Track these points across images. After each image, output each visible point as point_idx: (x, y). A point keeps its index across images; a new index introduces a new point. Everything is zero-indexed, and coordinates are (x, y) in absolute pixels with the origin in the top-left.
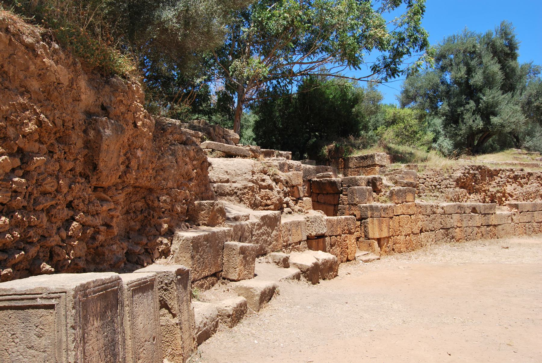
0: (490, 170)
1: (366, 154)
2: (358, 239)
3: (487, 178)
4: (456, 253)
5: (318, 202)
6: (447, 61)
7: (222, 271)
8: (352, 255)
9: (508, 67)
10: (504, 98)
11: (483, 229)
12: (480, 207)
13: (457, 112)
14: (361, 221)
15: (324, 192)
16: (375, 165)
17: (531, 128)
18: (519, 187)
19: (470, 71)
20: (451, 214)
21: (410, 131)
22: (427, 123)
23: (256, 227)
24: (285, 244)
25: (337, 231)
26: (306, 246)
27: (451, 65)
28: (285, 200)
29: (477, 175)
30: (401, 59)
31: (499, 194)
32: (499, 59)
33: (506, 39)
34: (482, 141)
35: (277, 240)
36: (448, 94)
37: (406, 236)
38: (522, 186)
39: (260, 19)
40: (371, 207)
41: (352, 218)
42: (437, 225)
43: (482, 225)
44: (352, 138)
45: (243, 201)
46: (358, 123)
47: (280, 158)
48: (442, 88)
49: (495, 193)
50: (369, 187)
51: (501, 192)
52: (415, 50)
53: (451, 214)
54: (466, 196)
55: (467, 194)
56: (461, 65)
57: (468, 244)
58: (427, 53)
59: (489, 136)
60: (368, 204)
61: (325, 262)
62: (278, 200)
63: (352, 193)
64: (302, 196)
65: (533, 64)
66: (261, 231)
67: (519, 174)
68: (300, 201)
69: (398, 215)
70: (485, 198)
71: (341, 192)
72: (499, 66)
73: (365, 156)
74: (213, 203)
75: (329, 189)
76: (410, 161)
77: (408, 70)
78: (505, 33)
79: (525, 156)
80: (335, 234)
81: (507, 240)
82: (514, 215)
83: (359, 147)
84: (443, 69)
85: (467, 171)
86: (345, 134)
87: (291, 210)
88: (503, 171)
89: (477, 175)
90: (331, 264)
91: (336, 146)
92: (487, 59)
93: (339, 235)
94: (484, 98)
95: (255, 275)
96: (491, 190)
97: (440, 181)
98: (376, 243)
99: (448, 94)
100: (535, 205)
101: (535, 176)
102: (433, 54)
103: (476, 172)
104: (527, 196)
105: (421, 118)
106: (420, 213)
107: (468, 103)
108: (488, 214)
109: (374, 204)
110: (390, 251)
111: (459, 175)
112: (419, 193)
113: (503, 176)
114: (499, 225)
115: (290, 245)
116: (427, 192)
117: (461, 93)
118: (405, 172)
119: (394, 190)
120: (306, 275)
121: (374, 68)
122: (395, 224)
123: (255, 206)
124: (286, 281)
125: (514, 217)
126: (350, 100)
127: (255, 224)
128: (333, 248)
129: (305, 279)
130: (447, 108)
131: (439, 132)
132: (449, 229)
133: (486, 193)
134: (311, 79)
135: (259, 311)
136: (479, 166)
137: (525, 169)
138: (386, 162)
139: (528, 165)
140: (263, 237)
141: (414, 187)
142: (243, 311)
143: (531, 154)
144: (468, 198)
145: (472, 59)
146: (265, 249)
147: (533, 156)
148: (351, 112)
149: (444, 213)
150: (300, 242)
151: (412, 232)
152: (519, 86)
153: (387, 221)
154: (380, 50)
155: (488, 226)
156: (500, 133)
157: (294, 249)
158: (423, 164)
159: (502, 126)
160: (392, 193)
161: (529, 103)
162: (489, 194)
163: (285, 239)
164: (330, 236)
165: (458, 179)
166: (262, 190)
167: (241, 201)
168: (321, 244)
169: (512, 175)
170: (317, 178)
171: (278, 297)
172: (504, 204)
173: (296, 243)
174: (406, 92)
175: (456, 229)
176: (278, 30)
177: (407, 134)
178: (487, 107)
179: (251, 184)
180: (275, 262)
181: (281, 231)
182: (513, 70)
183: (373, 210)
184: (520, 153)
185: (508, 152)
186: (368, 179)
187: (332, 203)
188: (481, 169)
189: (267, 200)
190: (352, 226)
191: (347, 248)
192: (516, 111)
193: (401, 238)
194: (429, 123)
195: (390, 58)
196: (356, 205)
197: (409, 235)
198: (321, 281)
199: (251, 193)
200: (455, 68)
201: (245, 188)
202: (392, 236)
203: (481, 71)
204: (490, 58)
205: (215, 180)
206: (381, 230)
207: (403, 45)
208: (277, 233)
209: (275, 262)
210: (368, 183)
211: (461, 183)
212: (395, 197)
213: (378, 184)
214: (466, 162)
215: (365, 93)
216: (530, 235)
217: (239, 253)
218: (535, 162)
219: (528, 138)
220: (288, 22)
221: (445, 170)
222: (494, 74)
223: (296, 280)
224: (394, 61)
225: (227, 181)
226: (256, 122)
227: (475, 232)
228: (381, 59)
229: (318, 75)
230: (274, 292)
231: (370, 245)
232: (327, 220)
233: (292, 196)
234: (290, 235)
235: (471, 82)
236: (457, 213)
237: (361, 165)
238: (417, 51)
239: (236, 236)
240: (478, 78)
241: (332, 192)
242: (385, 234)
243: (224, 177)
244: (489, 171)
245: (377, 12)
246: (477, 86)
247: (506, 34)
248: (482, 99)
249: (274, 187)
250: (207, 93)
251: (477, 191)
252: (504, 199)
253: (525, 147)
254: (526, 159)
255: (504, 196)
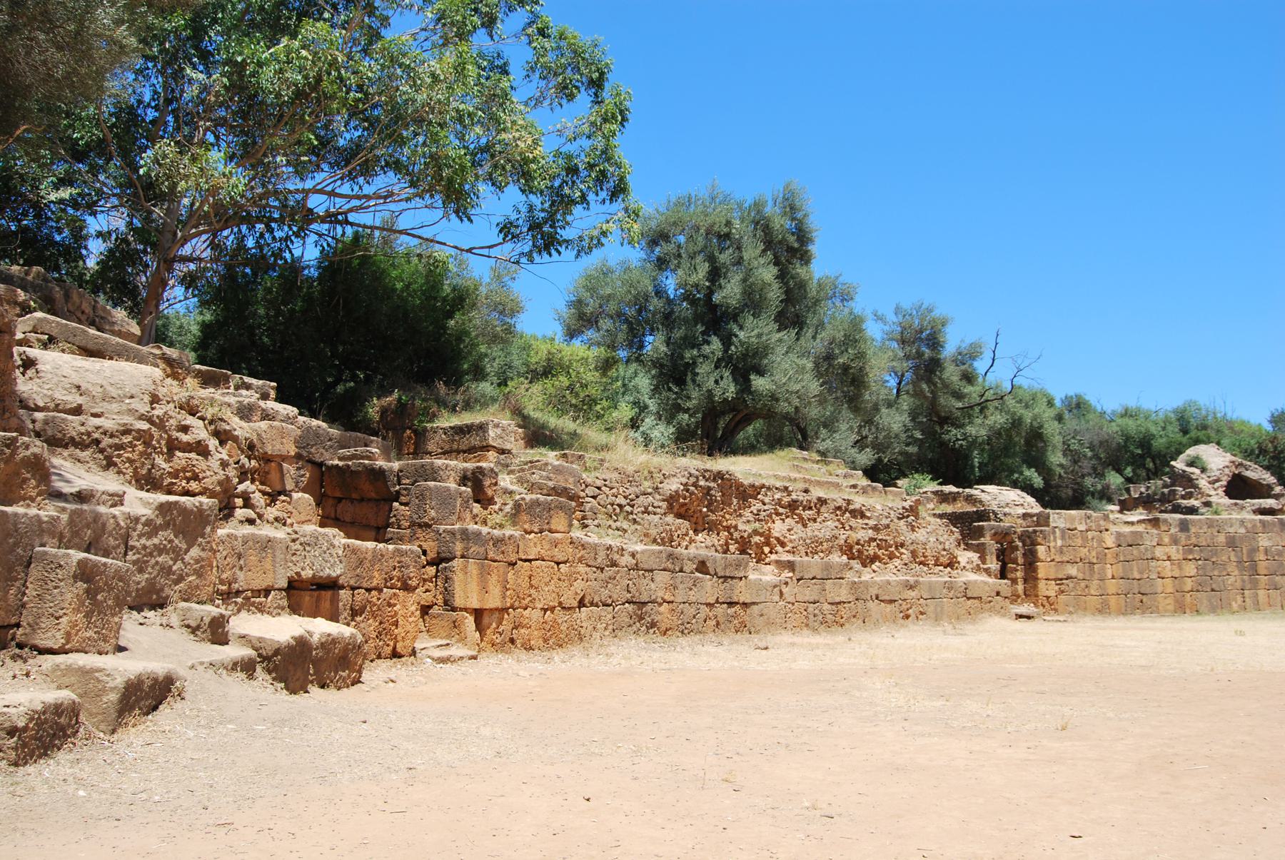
0: (742, 485)
1: (469, 422)
2: (425, 610)
3: (735, 501)
4: (656, 655)
5: (337, 519)
6: (671, 248)
7: (18, 625)
8: (408, 642)
9: (792, 277)
10: (780, 340)
11: (720, 610)
12: (715, 561)
13: (682, 358)
14: (438, 565)
15: (354, 496)
16: (487, 448)
17: (832, 413)
18: (800, 526)
19: (715, 274)
20: (652, 571)
21: (582, 395)
22: (619, 383)
23: (140, 527)
24: (224, 588)
25: (372, 578)
26: (285, 603)
27: (679, 256)
28: (241, 488)
29: (713, 492)
30: (569, 218)
31: (757, 539)
32: (776, 257)
33: (793, 219)
34: (732, 431)
35: (199, 574)
36: (668, 319)
37: (545, 610)
38: (805, 526)
39: (239, 59)
40: (464, 532)
41: (412, 552)
42: (618, 592)
43: (717, 602)
44: (442, 388)
45: (115, 465)
46: (458, 356)
47: (244, 392)
48: (655, 304)
49: (750, 536)
50: (463, 488)
51: (761, 535)
52: (600, 198)
53: (652, 571)
54: (687, 535)
55: (691, 532)
56: (699, 258)
57: (683, 641)
58: (626, 210)
59: (747, 420)
60: (457, 526)
61: (329, 643)
62: (220, 483)
63: (422, 497)
64: (289, 485)
65: (841, 279)
66: (156, 541)
67: (801, 498)
68: (282, 498)
69: (530, 561)
70: (727, 544)
71: (396, 497)
72: (774, 270)
73: (467, 426)
74: (15, 440)
75: (368, 489)
76: (570, 447)
77: (581, 238)
78: (791, 208)
79: (815, 466)
80: (365, 585)
81: (769, 637)
82: (786, 583)
83: (455, 406)
84: (662, 263)
85: (692, 480)
86: (426, 378)
87: (254, 516)
88: (769, 489)
89: (713, 492)
90: (346, 650)
91: (400, 399)
92: (752, 251)
93: (375, 589)
94: (742, 335)
95: (121, 649)
96: (741, 527)
97: (632, 496)
98: (470, 620)
99: (668, 319)
100: (828, 567)
101: (832, 506)
102: (637, 216)
103: (712, 485)
104: (814, 547)
105: (606, 366)
106: (580, 561)
107: (708, 343)
108: (732, 578)
109: (472, 527)
110: (503, 644)
111: (674, 487)
112: (584, 518)
113: (767, 500)
114: (754, 603)
115: (238, 593)
116: (602, 519)
117: (697, 319)
118: (554, 467)
119: (523, 499)
120: (271, 666)
121: (505, 226)
122: (520, 581)
123: (149, 482)
124: (211, 672)
125: (785, 590)
126: (444, 299)
127: (137, 520)
128: (358, 619)
129: (268, 677)
130: (663, 348)
131: (646, 407)
132: (645, 603)
133: (731, 534)
134: (357, 236)
135: (113, 731)
136: (719, 472)
137: (811, 489)
138: (514, 442)
139: (819, 483)
140: (160, 559)
141: (571, 498)
142: (63, 729)
143: (827, 463)
144: (692, 541)
145: (722, 250)
146: (162, 590)
147: (830, 468)
148: (445, 328)
149: (636, 567)
150: (267, 592)
151: (560, 603)
152: (811, 320)
153: (502, 570)
154: (523, 191)
155: (731, 604)
156: (769, 415)
157: (248, 605)
158: (598, 456)
159: (774, 398)
160: (517, 506)
161: (829, 357)
162: (736, 535)
163: (224, 576)
164: (353, 589)
165: (671, 497)
166: (178, 454)
167: (109, 464)
168: (326, 605)
169: (786, 500)
170: (340, 459)
171: (179, 705)
172: (767, 560)
173: (257, 593)
174: (578, 303)
175: (660, 605)
176: (278, 95)
177: (574, 401)
178: (745, 356)
179: (144, 426)
180: (188, 626)
181: (215, 552)
182: (802, 285)
183: (468, 539)
184: (805, 459)
185: (781, 453)
186: (465, 470)
187: (373, 523)
188: (722, 479)
189: (188, 480)
190: (412, 571)
191: (396, 624)
192: (802, 370)
193: (534, 615)
194: (624, 385)
195: (543, 210)
196: (428, 526)
197: (552, 609)
198: (314, 690)
199: (141, 448)
200: (685, 263)
201: (127, 432)
202: (512, 607)
203: (738, 277)
204: (758, 251)
205: (41, 404)
206: (485, 589)
207: (573, 182)
208: (203, 555)
209: (188, 626)
210: (463, 480)
211: (678, 506)
212: (524, 517)
213: (487, 482)
214: (694, 463)
215: (483, 290)
216: (815, 630)
217: (75, 577)
218: (833, 479)
219: (823, 431)
220: (306, 77)
221: (646, 473)
222: (765, 285)
223: (243, 676)
224: (551, 218)
225: (77, 411)
226: (205, 327)
227: (701, 616)
228: (524, 209)
229: (373, 228)
230: (170, 691)
231: (455, 625)
232: (346, 547)
233: (262, 483)
234: (241, 569)
235: (717, 298)
236: (664, 570)
237: (455, 446)
238: (604, 201)
239: (77, 540)
240: (730, 292)
241: (373, 495)
242: (493, 601)
243: (69, 398)
244: (739, 485)
245: (526, 104)
246: (728, 307)
247: (793, 208)
248: (736, 336)
249: (211, 448)
250: (79, 236)
251: (712, 527)
252: (767, 550)
253: (818, 452)
254: (817, 471)
255: (768, 543)
